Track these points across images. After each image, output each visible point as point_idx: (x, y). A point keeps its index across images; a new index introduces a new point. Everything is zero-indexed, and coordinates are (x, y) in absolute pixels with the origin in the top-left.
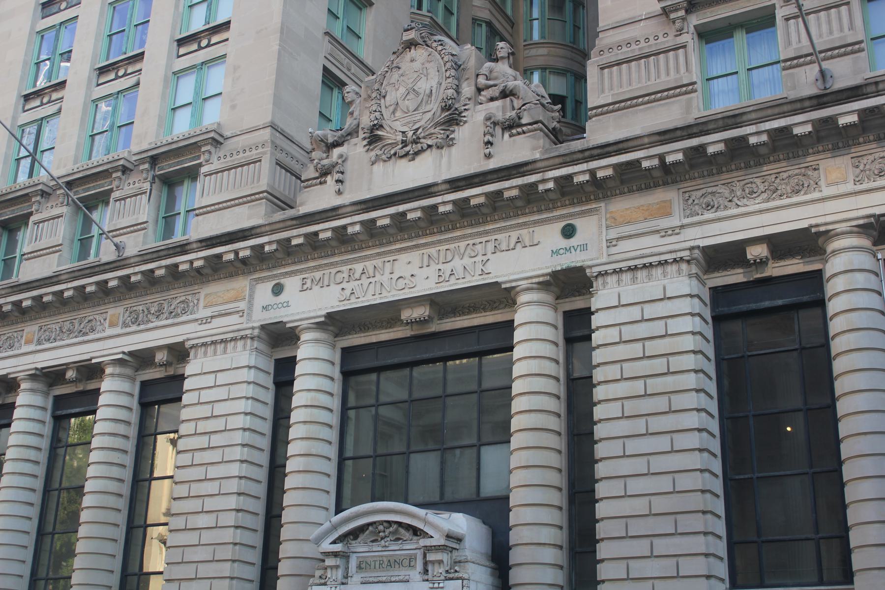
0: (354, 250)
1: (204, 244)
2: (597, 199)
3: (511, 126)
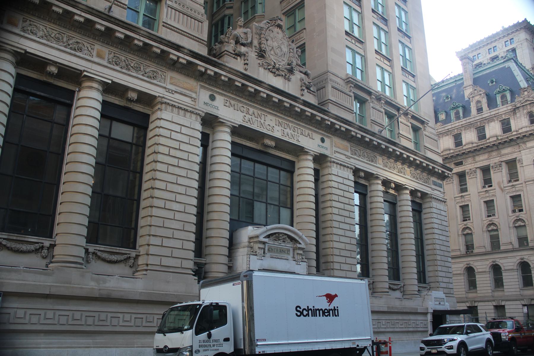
0: (251, 101)
1: (191, 53)
2: (331, 134)
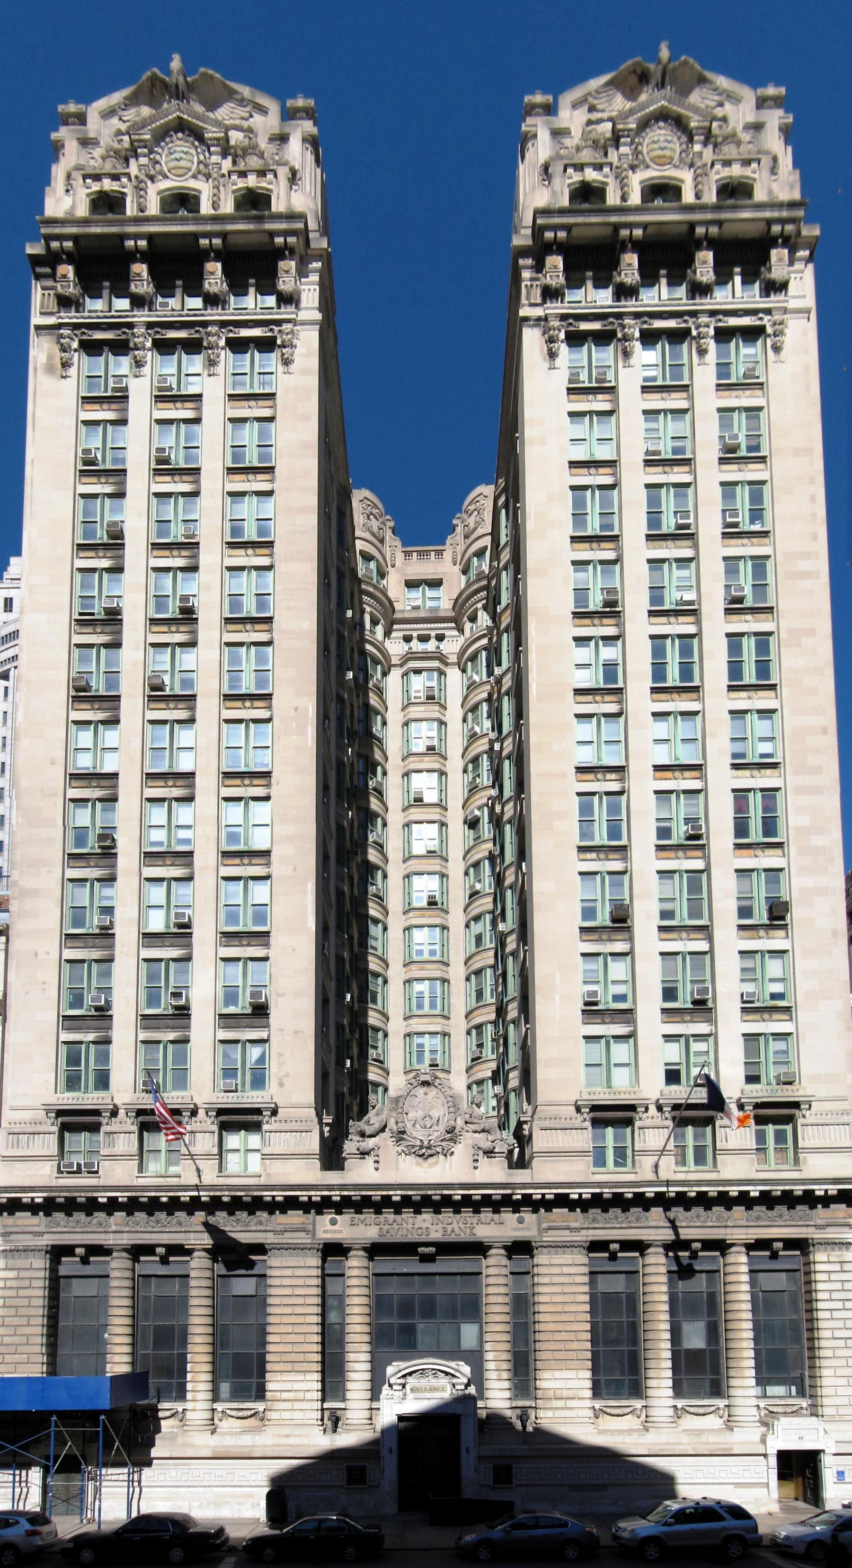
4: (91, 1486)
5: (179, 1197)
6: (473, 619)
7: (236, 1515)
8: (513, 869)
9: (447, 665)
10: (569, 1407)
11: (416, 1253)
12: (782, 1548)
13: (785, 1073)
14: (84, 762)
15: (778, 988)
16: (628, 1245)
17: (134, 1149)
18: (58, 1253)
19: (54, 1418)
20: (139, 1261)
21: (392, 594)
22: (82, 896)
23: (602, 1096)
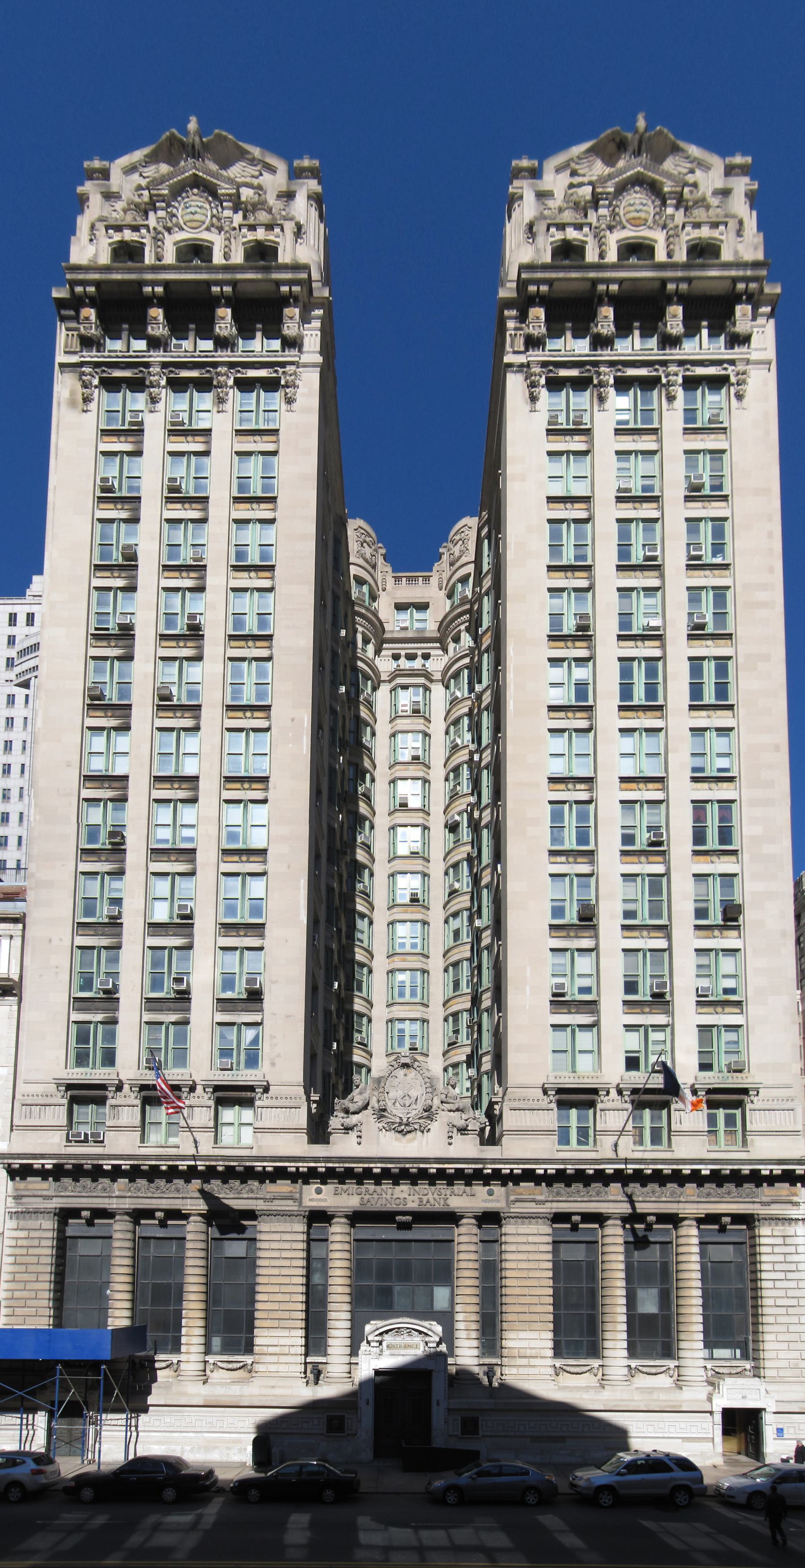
3: (463, 1130)
4: (92, 1429)
5: (177, 1166)
6: (457, 640)
7: (225, 1459)
8: (489, 870)
9: (432, 681)
10: (532, 1364)
11: (393, 1221)
12: (725, 1498)
13: (735, 1062)
14: (98, 765)
15: (730, 983)
16: (588, 1217)
17: (137, 1121)
18: (65, 1215)
19: (59, 1367)
20: (139, 1224)
21: (382, 616)
22: (93, 888)
23: (567, 1080)
